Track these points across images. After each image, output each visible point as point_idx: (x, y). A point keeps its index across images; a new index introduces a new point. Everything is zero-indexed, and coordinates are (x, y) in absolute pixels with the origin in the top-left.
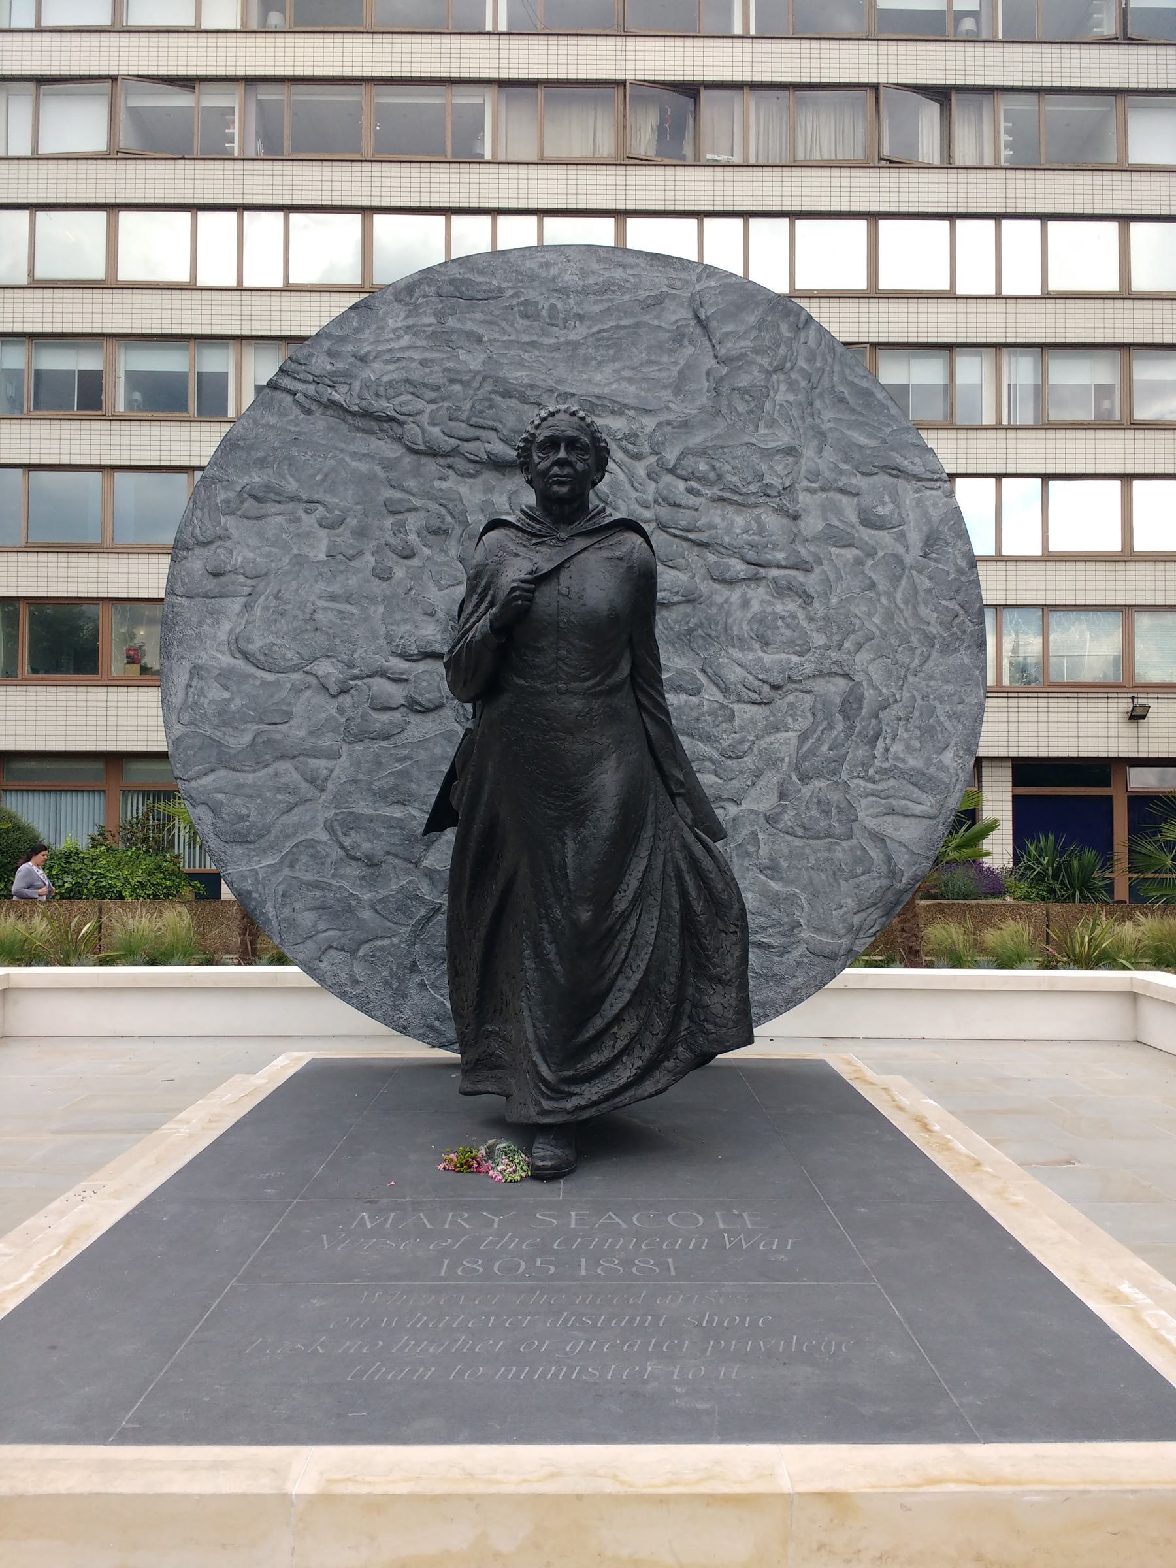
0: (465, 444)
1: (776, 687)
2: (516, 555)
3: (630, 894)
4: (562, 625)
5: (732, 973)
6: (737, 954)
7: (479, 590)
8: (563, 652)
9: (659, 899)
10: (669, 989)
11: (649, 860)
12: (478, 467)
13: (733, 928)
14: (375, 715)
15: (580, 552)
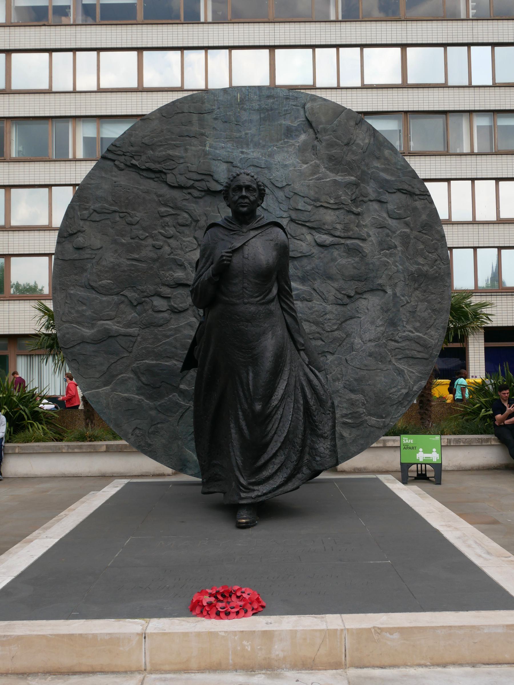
0: (197, 183)
1: (349, 297)
2: (223, 240)
3: (279, 397)
4: (245, 272)
5: (328, 433)
6: (330, 424)
7: (206, 256)
8: (246, 285)
9: (293, 399)
10: (299, 441)
11: (288, 381)
12: (203, 194)
13: (328, 412)
14: (156, 315)
15: (252, 238)
